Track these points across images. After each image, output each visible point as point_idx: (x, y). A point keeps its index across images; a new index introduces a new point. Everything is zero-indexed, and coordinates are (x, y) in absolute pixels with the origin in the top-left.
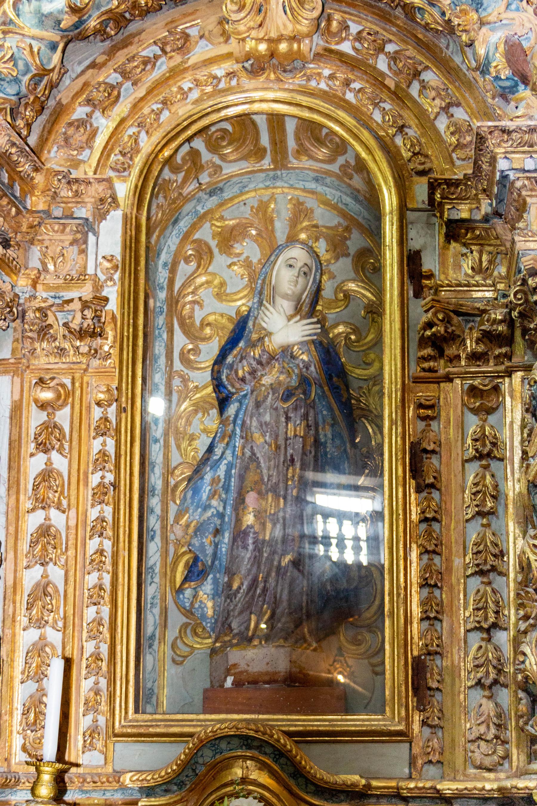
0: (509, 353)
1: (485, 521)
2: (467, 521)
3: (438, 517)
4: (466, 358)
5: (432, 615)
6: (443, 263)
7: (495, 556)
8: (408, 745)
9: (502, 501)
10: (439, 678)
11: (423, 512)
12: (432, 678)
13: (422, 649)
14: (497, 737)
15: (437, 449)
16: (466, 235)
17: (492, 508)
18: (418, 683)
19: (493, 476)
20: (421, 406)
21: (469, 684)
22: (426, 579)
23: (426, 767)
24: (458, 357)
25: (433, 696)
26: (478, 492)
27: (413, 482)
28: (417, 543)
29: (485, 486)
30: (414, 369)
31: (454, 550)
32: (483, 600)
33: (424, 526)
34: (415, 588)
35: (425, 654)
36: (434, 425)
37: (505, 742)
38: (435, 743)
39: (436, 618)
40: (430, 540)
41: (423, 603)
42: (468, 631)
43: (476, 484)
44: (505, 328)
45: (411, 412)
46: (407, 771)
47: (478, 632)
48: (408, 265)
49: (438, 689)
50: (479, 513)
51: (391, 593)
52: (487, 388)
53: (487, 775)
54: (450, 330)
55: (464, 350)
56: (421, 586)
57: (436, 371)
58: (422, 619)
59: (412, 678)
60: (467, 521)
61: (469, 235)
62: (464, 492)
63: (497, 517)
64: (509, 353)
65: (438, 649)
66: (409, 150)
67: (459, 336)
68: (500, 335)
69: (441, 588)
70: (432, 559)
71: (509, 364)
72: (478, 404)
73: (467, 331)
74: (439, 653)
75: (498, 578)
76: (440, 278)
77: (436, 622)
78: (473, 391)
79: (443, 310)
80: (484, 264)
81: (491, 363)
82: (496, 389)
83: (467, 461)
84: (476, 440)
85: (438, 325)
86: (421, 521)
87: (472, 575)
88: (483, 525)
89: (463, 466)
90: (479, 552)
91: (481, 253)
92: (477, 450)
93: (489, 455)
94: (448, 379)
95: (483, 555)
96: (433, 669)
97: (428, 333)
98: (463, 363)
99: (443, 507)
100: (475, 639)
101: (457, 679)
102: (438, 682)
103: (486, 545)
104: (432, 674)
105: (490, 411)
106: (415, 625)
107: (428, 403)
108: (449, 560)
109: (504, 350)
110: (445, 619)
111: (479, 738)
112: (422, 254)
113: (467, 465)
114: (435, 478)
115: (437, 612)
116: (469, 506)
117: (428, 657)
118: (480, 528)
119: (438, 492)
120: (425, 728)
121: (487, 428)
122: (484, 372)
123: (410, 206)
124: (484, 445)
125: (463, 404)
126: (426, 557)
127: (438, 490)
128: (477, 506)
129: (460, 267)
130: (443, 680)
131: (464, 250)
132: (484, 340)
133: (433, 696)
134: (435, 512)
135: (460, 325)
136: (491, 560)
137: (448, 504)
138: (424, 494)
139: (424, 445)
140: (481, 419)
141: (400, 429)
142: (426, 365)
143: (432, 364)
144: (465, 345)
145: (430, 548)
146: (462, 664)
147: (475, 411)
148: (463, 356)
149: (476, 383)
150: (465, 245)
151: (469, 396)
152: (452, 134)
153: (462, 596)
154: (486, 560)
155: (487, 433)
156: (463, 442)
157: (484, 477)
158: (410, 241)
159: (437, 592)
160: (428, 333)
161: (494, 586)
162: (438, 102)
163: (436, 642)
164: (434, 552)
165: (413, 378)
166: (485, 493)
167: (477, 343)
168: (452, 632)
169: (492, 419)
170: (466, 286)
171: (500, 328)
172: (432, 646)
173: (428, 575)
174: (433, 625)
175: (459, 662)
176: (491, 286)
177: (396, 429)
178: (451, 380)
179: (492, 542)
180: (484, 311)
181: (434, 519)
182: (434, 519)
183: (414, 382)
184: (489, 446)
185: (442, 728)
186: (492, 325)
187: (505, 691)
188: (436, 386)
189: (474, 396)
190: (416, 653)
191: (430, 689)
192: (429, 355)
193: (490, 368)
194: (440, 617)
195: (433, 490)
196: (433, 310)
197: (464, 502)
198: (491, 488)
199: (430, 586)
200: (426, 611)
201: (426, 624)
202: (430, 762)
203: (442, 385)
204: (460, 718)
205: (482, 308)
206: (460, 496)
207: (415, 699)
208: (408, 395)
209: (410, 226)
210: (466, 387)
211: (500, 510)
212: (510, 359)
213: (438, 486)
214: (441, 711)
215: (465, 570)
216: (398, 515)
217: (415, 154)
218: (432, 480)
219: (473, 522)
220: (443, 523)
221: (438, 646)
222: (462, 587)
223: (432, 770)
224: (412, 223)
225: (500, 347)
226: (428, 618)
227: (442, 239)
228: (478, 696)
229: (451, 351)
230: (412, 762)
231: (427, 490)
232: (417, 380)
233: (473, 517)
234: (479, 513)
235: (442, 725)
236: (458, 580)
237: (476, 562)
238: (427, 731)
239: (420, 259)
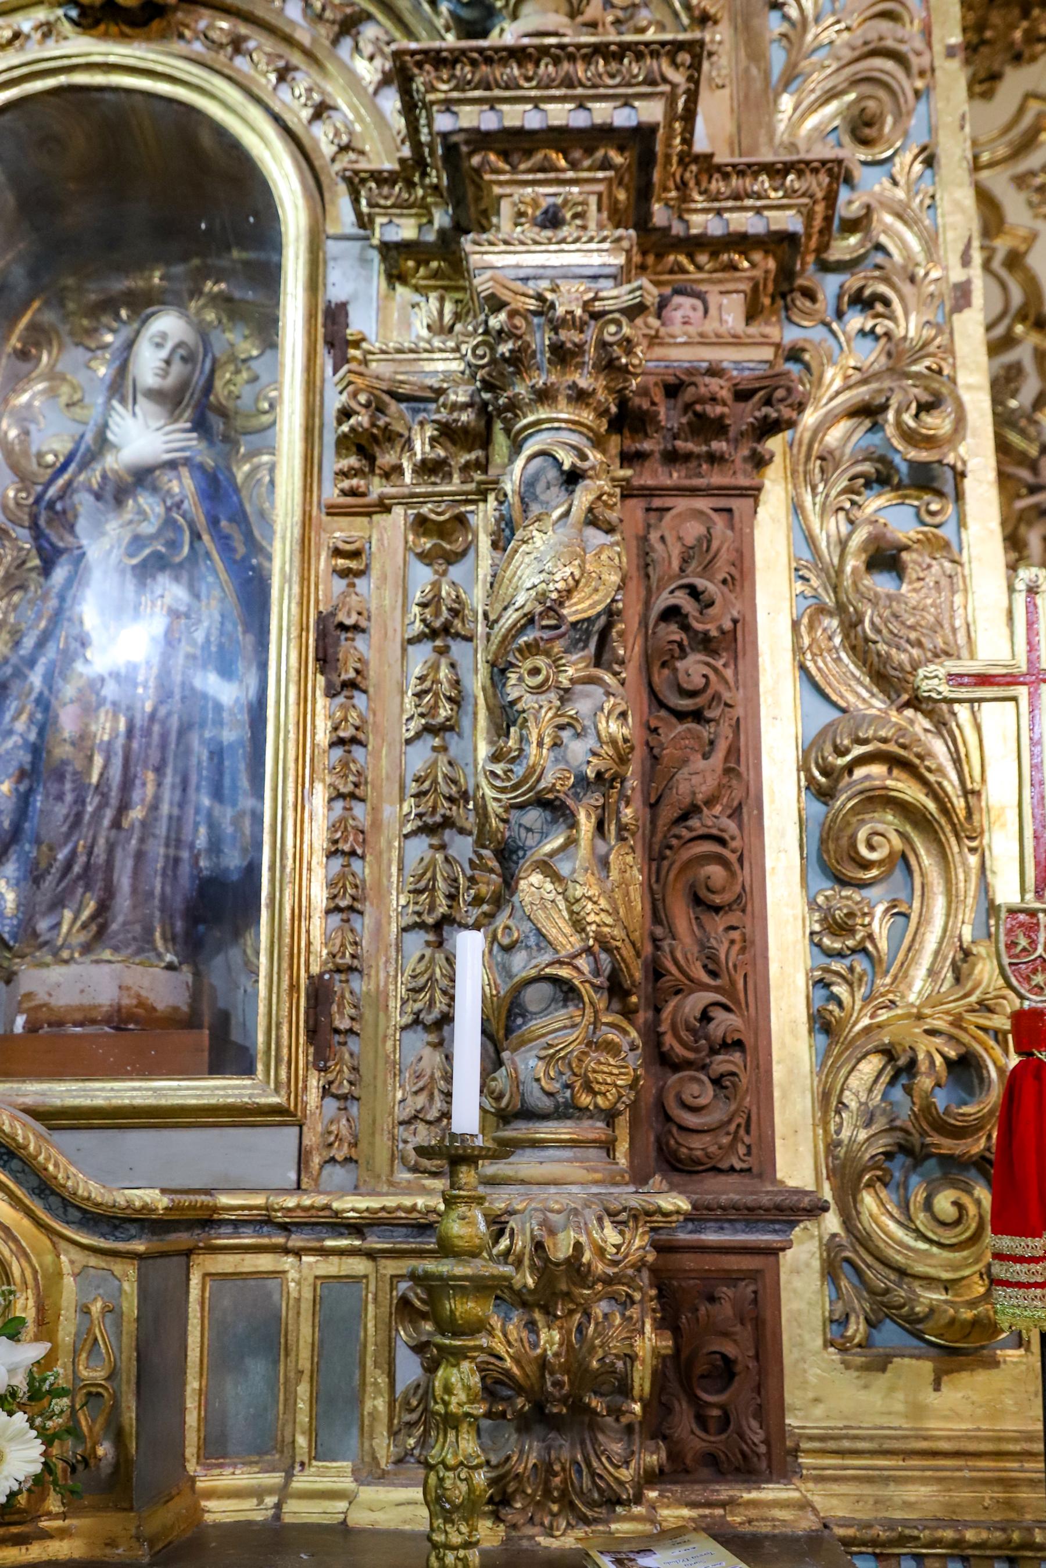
0: (483, 460)
1: (437, 742)
2: (408, 742)
3: (361, 736)
4: (414, 471)
5: (343, 904)
6: (383, 321)
7: (450, 799)
9: (470, 709)
10: (353, 1012)
11: (335, 729)
12: (341, 1013)
13: (326, 963)
15: (363, 623)
16: (417, 271)
17: (448, 719)
18: (317, 1021)
19: (453, 666)
20: (337, 553)
22: (335, 842)
24: (398, 469)
25: (345, 1044)
26: (426, 692)
28: (323, 781)
29: (436, 681)
30: (331, 493)
31: (385, 790)
34: (319, 858)
35: (331, 971)
39: (351, 908)
40: (346, 776)
41: (330, 885)
42: (405, 930)
43: (422, 679)
44: (473, 417)
45: (323, 563)
48: (325, 326)
49: (351, 1031)
50: (428, 729)
51: (272, 868)
52: (442, 518)
54: (381, 423)
55: (410, 458)
56: (330, 855)
57: (363, 495)
58: (328, 912)
59: (307, 1013)
60: (408, 742)
61: (422, 271)
62: (403, 693)
63: (460, 735)
64: (483, 460)
65: (356, 963)
67: (401, 436)
68: (465, 429)
69: (362, 857)
71: (483, 477)
72: (428, 546)
73: (416, 427)
74: (356, 969)
76: (374, 344)
77: (354, 916)
79: (370, 389)
81: (456, 478)
82: (461, 520)
83: (411, 641)
84: (424, 605)
87: (414, 833)
88: (434, 749)
89: (404, 650)
90: (424, 793)
91: (442, 300)
92: (423, 621)
93: (446, 630)
94: (384, 507)
95: (430, 799)
96: (343, 997)
97: (345, 428)
98: (408, 477)
99: (371, 719)
100: (416, 943)
102: (352, 1019)
103: (435, 782)
104: (341, 1006)
105: (452, 558)
107: (348, 547)
108: (376, 810)
109: (473, 456)
110: (368, 908)
112: (351, 310)
113: (411, 649)
115: (354, 898)
116: (411, 718)
117: (337, 977)
118: (431, 755)
120: (328, 1100)
122: (442, 494)
123: (331, 230)
124: (437, 614)
125: (407, 549)
126: (339, 805)
128: (422, 715)
129: (409, 325)
130: (361, 1016)
131: (417, 298)
133: (345, 1044)
134: (357, 728)
135: (401, 417)
136: (444, 808)
137: (379, 714)
139: (342, 617)
140: (436, 572)
141: (296, 589)
142: (346, 484)
143: (355, 482)
144: (411, 449)
145: (343, 790)
147: (425, 557)
148: (407, 466)
149: (425, 510)
150: (417, 289)
151: (417, 535)
153: (394, 870)
154: (434, 808)
155: (444, 594)
157: (436, 667)
158: (330, 288)
159: (356, 865)
160: (345, 428)
161: (451, 852)
163: (350, 950)
164: (353, 796)
165: (330, 507)
166: (436, 695)
167: (432, 447)
170: (412, 351)
171: (464, 417)
172: (343, 956)
173: (338, 835)
174: (348, 921)
178: (387, 510)
179: (445, 776)
180: (440, 392)
181: (354, 740)
182: (354, 740)
183: (328, 514)
184: (445, 614)
185: (358, 1099)
186: (451, 412)
189: (426, 534)
190: (315, 969)
192: (351, 468)
194: (358, 906)
196: (351, 388)
197: (402, 710)
198: (446, 685)
199: (343, 853)
200: (334, 897)
201: (336, 919)
205: (436, 385)
206: (398, 699)
207: (311, 1050)
208: (318, 534)
209: (331, 264)
211: (466, 723)
212: (485, 471)
215: (402, 825)
216: (287, 732)
218: (352, 674)
219: (419, 745)
221: (353, 956)
222: (395, 854)
224: (335, 259)
225: (470, 451)
226: (338, 909)
227: (384, 284)
228: (419, 1044)
229: (386, 459)
232: (334, 511)
233: (418, 735)
234: (428, 729)
237: (421, 810)
239: (347, 315)
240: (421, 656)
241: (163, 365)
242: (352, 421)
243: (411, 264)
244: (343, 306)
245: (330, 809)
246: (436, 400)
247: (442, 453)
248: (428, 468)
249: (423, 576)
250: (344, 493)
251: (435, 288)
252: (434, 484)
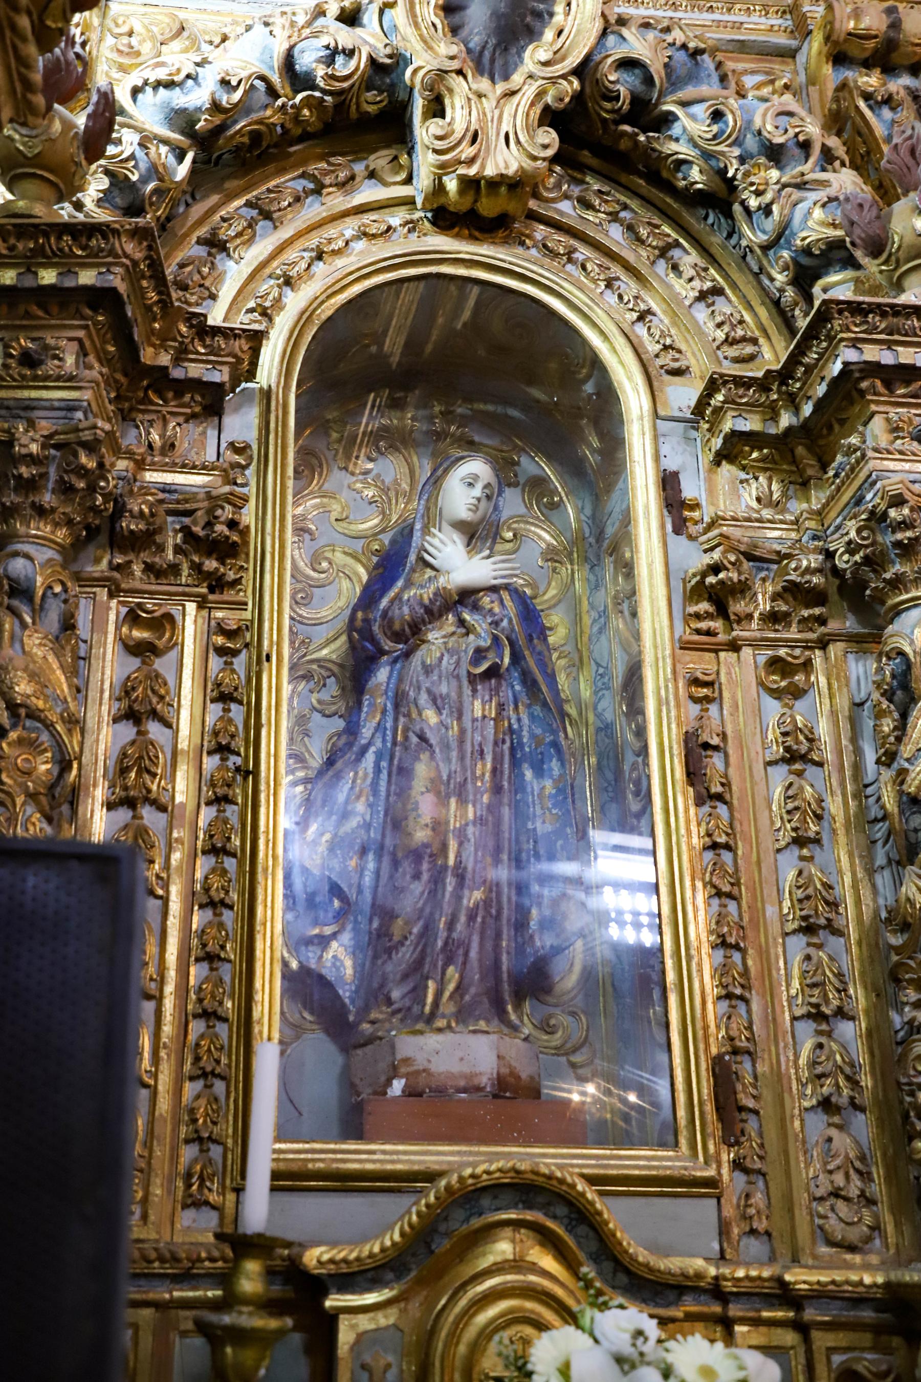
2: (779, 851)
8: (714, 1201)
11: (709, 835)
14: (862, 1194)
21: (806, 1104)
23: (745, 1241)
27: (691, 790)
32: (820, 971)
33: (709, 855)
35: (728, 1053)
36: (713, 709)
37: (871, 1202)
38: (758, 1198)
46: (716, 1246)
47: (810, 1021)
52: (797, 662)
53: (848, 1257)
56: (714, 947)
60: (779, 851)
66: (658, 342)
70: (725, 906)
75: (832, 939)
78: (775, 664)
80: (775, 497)
82: (807, 666)
85: (728, 570)
86: (706, 848)
87: (794, 932)
91: (770, 480)
94: (734, 647)
97: (711, 580)
101: (786, 1095)
106: (710, 1006)
107: (706, 678)
109: (817, 611)
111: (836, 1194)
114: (723, 785)
119: (725, 807)
121: (798, 718)
127: (726, 803)
132: (785, 595)
137: (745, 824)
138: (706, 809)
139: (705, 737)
142: (704, 625)
146: (792, 1071)
147: (776, 694)
149: (782, 652)
152: (719, 325)
153: (781, 963)
156: (764, 736)
160: (711, 580)
162: (697, 284)
164: (730, 896)
168: (772, 1020)
169: (799, 705)
171: (815, 580)
175: (787, 1069)
176: (792, 523)
177: (669, 712)
180: (789, 556)
182: (727, 847)
183: (681, 648)
186: (802, 575)
187: (861, 1117)
188: (713, 655)
190: (714, 1051)
191: (741, 1109)
192: (706, 612)
193: (793, 633)
195: (718, 804)
197: (772, 823)
201: (725, 1004)
202: (753, 1232)
203: (722, 655)
204: (797, 1158)
210: (762, 660)
213: (727, 797)
214: (762, 1146)
217: (666, 348)
218: (719, 789)
220: (740, 852)
223: (754, 1246)
229: (738, 607)
230: (723, 1230)
231: (708, 803)
235: (764, 1169)
236: (775, 939)
238: (740, 1178)
240: (780, 776)
241: (475, 501)
242: (722, 575)
243: (747, 448)
244: (675, 475)
245: (709, 905)
246: (778, 562)
247: (784, 608)
248: (773, 618)
249: (773, 708)
250: (698, 632)
251: (765, 470)
252: (776, 631)
